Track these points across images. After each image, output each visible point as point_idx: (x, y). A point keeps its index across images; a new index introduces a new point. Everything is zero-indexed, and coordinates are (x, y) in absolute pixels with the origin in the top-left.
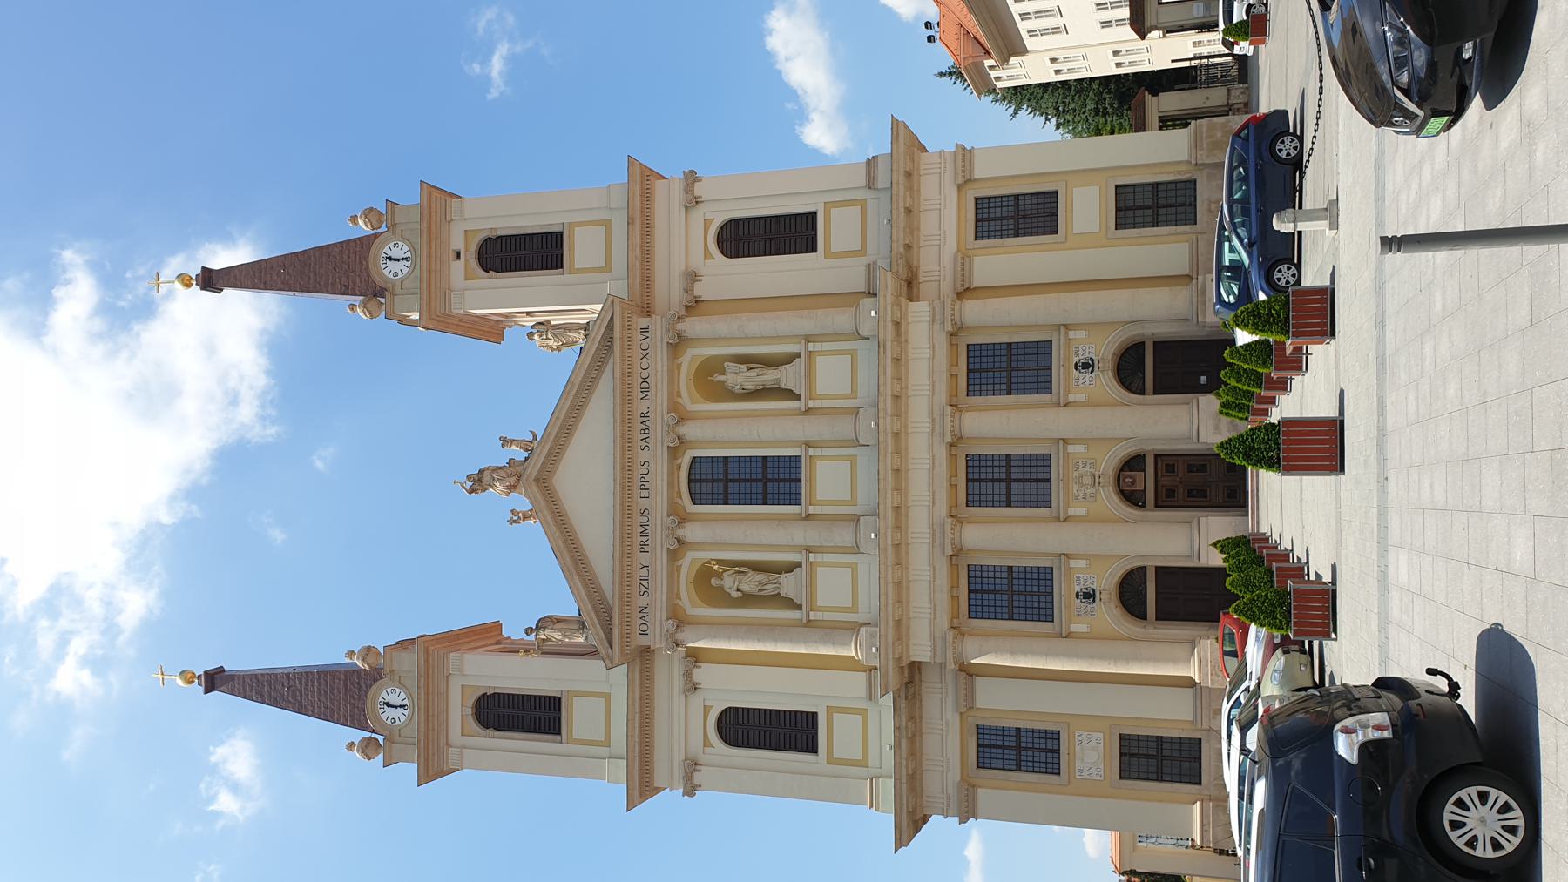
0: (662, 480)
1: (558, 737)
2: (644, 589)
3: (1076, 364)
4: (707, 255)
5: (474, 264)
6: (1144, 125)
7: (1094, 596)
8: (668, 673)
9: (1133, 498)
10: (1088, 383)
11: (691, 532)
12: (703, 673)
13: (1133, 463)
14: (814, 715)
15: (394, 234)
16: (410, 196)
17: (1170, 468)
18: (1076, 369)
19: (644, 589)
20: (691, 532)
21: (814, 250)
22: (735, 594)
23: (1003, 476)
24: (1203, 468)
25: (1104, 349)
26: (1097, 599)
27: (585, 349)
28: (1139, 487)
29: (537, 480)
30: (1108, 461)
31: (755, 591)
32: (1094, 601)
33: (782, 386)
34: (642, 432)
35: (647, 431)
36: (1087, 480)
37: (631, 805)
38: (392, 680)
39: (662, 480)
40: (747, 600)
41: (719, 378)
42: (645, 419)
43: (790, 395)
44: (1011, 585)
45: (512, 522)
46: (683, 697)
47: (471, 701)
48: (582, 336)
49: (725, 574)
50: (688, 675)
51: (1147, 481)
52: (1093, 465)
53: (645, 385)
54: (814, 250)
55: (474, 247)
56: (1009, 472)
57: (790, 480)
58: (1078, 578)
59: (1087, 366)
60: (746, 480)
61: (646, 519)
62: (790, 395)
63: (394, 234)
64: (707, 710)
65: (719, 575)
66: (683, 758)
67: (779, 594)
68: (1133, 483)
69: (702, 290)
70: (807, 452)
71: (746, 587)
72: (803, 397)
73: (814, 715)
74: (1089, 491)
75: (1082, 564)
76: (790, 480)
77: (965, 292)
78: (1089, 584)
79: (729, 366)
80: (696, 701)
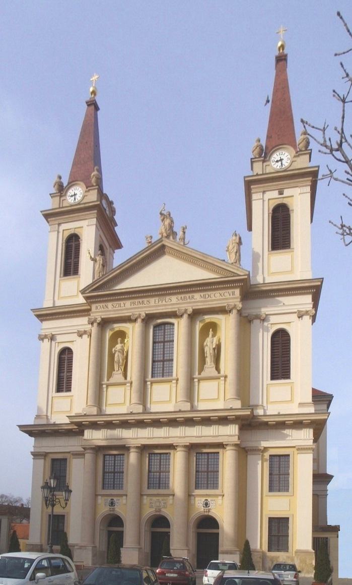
0: (162, 309)
6: (316, 531)
8: (81, 323)
22: (113, 350)
27: (224, 263)
36: (158, 504)
40: (112, 356)
41: (211, 333)
42: (191, 298)
44: (118, 472)
46: (76, 331)
48: (233, 261)
52: (165, 507)
53: (207, 296)
57: (163, 373)
59: (206, 504)
60: (164, 351)
72: (200, 376)
73: (70, 391)
75: (124, 501)
76: (163, 373)
79: (215, 339)
80: (75, 337)
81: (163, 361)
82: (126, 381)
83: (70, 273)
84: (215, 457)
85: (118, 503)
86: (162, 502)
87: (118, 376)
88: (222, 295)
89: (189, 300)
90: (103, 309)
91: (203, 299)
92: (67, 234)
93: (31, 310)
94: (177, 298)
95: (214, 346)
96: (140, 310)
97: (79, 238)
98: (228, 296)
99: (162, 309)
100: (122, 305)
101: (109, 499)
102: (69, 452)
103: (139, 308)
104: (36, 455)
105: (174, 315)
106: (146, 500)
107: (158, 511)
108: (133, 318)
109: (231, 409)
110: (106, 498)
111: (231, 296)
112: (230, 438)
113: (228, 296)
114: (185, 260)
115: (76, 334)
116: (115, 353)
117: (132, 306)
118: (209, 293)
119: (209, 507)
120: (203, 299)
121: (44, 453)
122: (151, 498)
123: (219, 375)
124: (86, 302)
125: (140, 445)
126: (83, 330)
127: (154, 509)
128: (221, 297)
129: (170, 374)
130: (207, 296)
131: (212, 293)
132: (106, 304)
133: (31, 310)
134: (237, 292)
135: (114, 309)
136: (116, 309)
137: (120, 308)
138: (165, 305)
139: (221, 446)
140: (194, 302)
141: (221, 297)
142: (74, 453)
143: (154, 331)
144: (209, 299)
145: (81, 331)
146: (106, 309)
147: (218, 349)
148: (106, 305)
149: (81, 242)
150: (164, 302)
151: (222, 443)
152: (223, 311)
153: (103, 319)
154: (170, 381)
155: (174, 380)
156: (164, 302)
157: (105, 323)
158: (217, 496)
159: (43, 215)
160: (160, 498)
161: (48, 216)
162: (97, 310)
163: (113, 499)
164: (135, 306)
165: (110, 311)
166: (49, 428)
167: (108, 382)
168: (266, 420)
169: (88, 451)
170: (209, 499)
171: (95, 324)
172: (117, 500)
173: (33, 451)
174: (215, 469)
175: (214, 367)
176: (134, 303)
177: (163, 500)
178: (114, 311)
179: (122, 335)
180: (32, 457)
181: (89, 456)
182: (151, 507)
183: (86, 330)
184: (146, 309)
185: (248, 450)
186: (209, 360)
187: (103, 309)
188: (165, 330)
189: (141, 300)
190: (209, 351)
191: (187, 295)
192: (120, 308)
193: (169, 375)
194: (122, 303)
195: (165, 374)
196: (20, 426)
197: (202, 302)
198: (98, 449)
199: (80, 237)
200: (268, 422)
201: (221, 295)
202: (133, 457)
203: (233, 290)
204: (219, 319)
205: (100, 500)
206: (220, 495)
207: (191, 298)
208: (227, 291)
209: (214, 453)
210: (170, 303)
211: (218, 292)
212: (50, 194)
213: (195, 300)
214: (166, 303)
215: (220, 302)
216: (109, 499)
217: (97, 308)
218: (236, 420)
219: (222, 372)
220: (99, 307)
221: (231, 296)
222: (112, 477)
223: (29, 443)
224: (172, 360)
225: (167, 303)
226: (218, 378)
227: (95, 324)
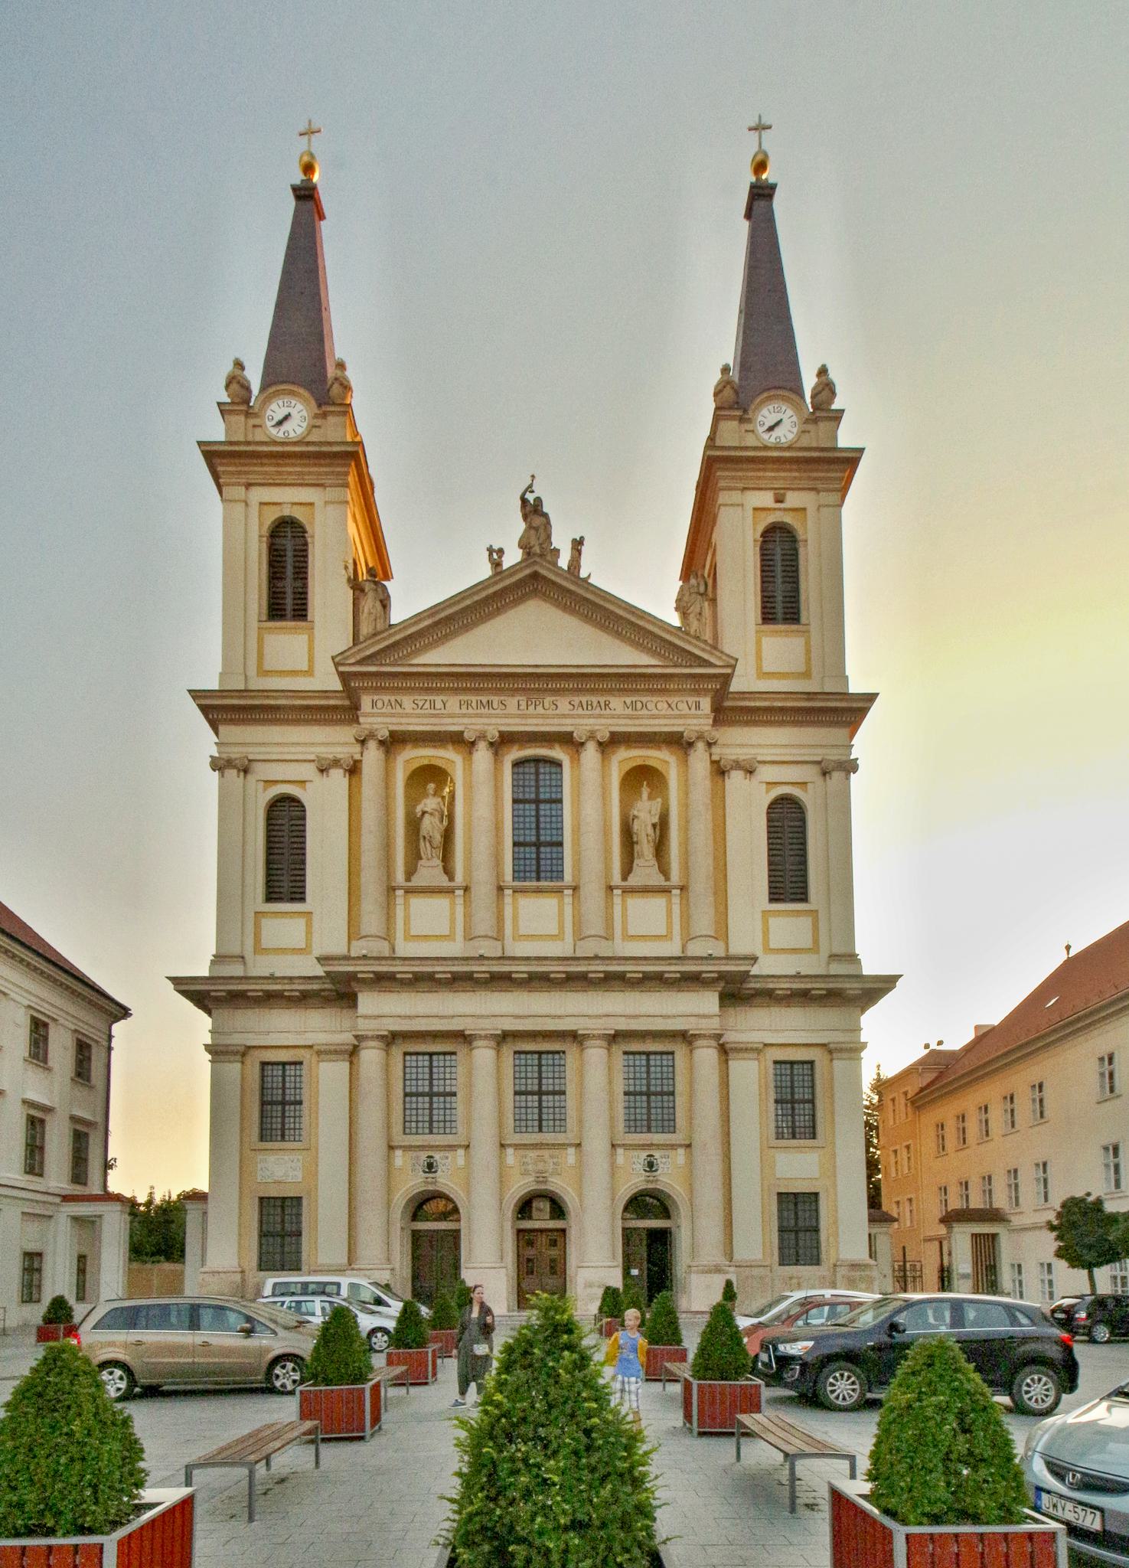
1: (264, 618)
2: (421, 704)
4: (771, 784)
5: (772, 518)
8: (335, 740)
9: (525, 1208)
11: (482, 755)
12: (338, 778)
13: (558, 1209)
14: (303, 900)
15: (807, 421)
16: (846, 438)
17: (553, 1243)
19: (421, 704)
20: (482, 755)
21: (772, 900)
22: (419, 809)
23: (544, 1088)
24: (553, 1271)
25: (670, 1178)
26: (427, 1175)
28: (535, 1214)
29: (535, 576)
30: (559, 1185)
31: (423, 832)
32: (425, 1172)
33: (636, 862)
36: (541, 1166)
37: (195, 694)
38: (316, 416)
40: (414, 825)
42: (603, 705)
43: (627, 871)
44: (439, 1094)
45: (490, 550)
47: (299, 514)
49: (440, 799)
50: (336, 763)
51: (541, 1220)
53: (639, 705)
54: (772, 900)
55: (788, 519)
56: (548, 1093)
57: (538, 872)
58: (447, 1158)
59: (651, 1166)
61: (495, 706)
62: (627, 871)
63: (807, 421)
64: (302, 783)
65: (437, 793)
66: (251, 757)
67: (421, 859)
68: (540, 1210)
69: (736, 778)
70: (568, 888)
71: (427, 819)
73: (303, 900)
74: (530, 1167)
75: (461, 1161)
76: (538, 872)
77: (724, 1051)
80: (308, 771)
82: (667, 883)
83: (285, 615)
87: (430, 872)
88: (674, 706)
89: (598, 711)
91: (629, 711)
92: (272, 515)
96: (486, 721)
97: (305, 532)
98: (686, 711)
99: (626, 725)
100: (439, 705)
101: (423, 1155)
102: (311, 1047)
103: (480, 716)
104: (216, 1052)
108: (469, 736)
109: (710, 957)
112: (704, 1021)
113: (686, 711)
114: (587, 619)
117: (464, 710)
118: (644, 699)
120: (629, 711)
121: (242, 1049)
122: (522, 1152)
123: (667, 883)
125: (499, 1032)
126: (331, 756)
128: (670, 712)
130: (639, 705)
131: (650, 700)
132: (399, 698)
134: (706, 703)
135: (419, 711)
136: (422, 712)
137: (433, 711)
138: (543, 716)
139: (685, 1037)
141: (670, 712)
142: (323, 1048)
144: (644, 712)
145: (326, 759)
146: (399, 710)
147: (662, 826)
149: (309, 540)
150: (540, 710)
151: (576, 1031)
153: (392, 734)
154: (559, 891)
155: (568, 888)
156: (540, 710)
160: (546, 1153)
162: (375, 710)
163: (431, 1157)
164: (470, 711)
165: (407, 716)
166: (258, 987)
167: (409, 884)
172: (441, 1158)
173: (209, 1042)
175: (441, 867)
176: (469, 704)
177: (552, 1157)
178: (418, 716)
180: (209, 1057)
182: (525, 1173)
183: (339, 756)
184: (499, 721)
190: (644, 830)
191: (594, 699)
192: (433, 711)
194: (438, 699)
195: (542, 875)
196: (178, 982)
199: (308, 528)
201: (670, 706)
207: (603, 705)
208: (684, 699)
210: (554, 712)
211: (664, 699)
213: (613, 712)
215: (672, 721)
216: (423, 1156)
217: (374, 704)
219: (459, 878)
220: (380, 704)
221: (693, 711)
222: (427, 1106)
223: (201, 1024)
225: (548, 712)
227: (372, 745)
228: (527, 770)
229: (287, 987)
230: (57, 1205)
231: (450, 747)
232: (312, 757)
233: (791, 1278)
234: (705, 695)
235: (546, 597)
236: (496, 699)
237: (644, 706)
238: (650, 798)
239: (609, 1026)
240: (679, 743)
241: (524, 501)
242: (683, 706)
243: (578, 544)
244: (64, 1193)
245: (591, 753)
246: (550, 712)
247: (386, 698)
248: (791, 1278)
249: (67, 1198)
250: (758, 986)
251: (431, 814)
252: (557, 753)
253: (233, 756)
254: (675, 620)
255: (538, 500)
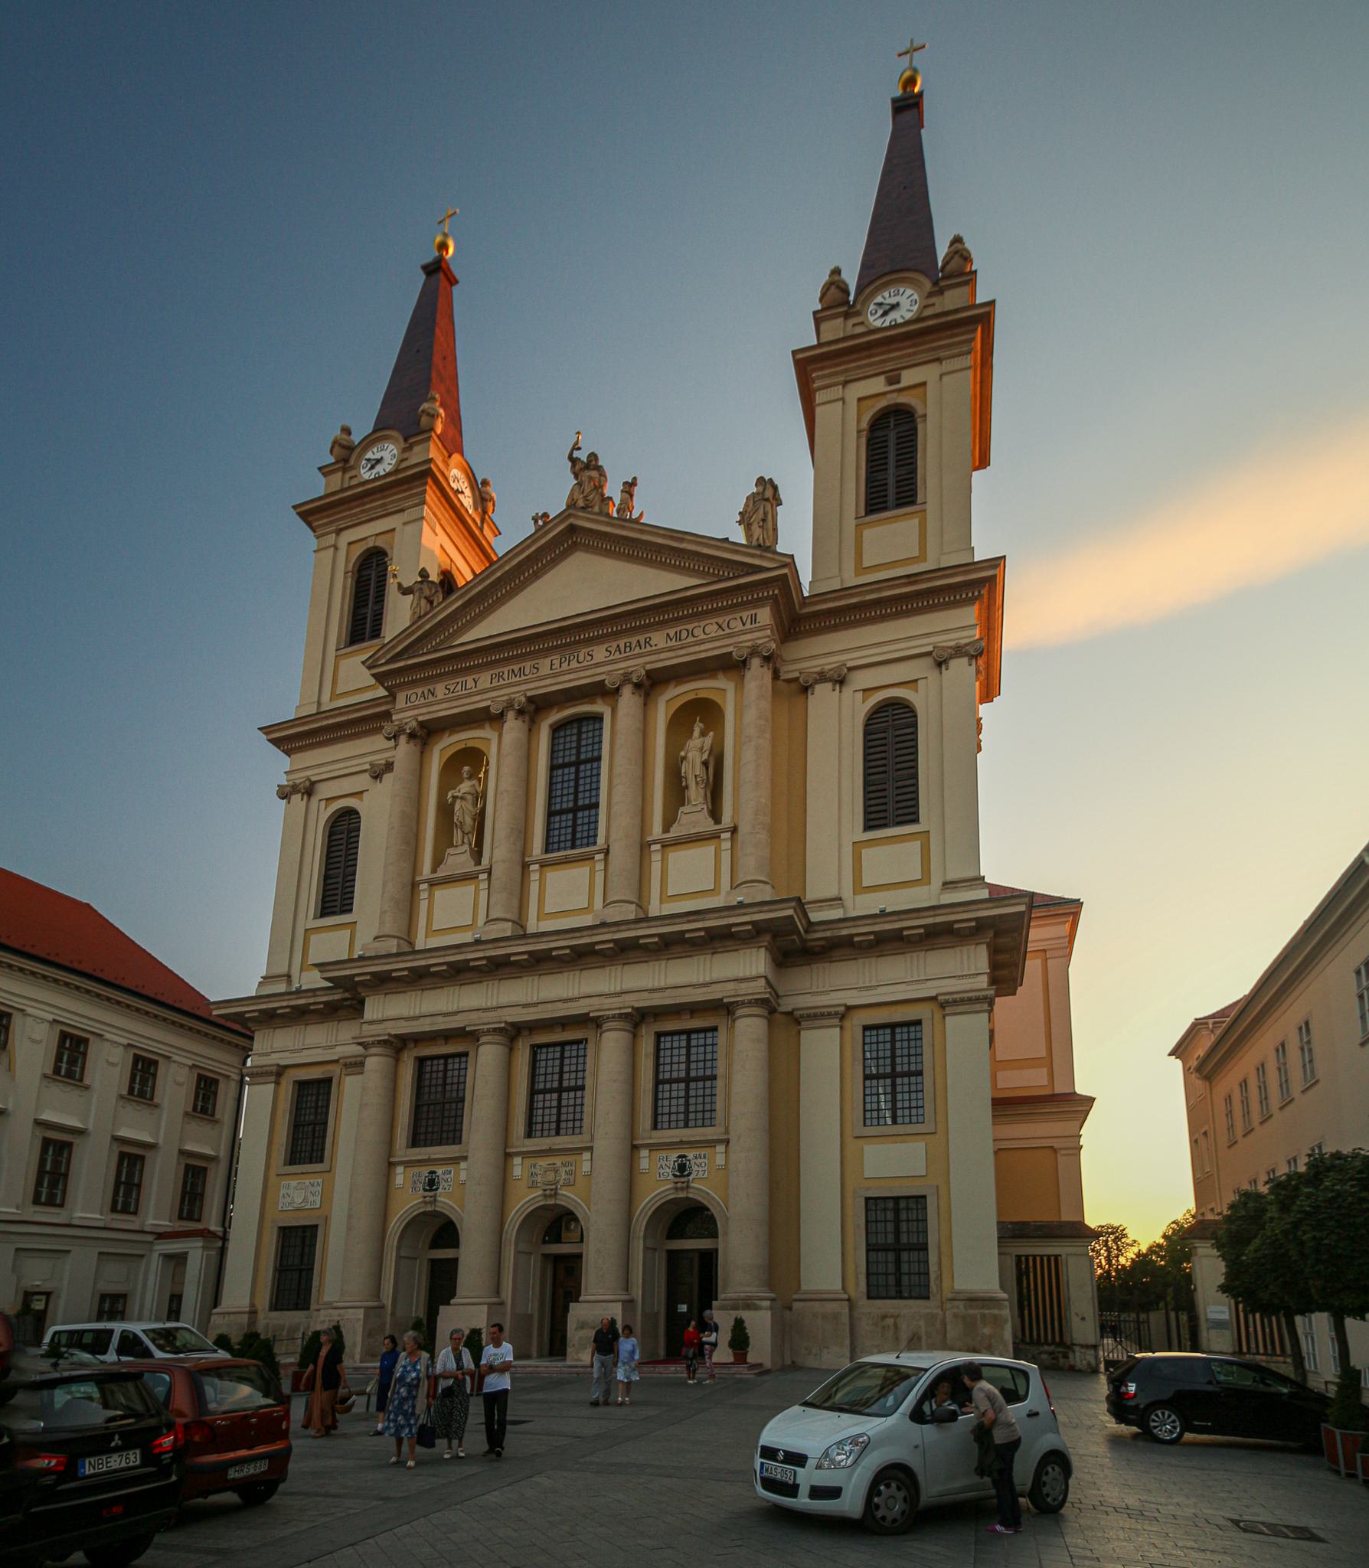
0: (570, 681)
3: (684, 1156)
7: (431, 1190)
10: (662, 1171)
18: (679, 1157)
22: (450, 794)
32: (425, 1190)
34: (628, 645)
35: (628, 649)
36: (551, 1176)
38: (404, 450)
39: (570, 681)
40: (445, 811)
52: (568, 1184)
57: (574, 840)
58: (450, 1173)
59: (682, 1168)
66: (313, 779)
76: (574, 840)
78: (443, 1184)
81: (575, 810)
84: (709, 1041)
85: (446, 1181)
86: (563, 1171)
88: (725, 626)
90: (422, 701)
91: (673, 643)
92: (358, 551)
93: (259, 729)
94: (607, 650)
95: (705, 756)
98: (740, 627)
101: (425, 1171)
102: (336, 1061)
105: (600, 691)
106: (518, 1167)
107: (550, 1196)
108: (495, 709)
110: (416, 1170)
111: (748, 626)
112: (743, 985)
113: (740, 627)
115: (367, 775)
116: (453, 804)
118: (690, 627)
119: (689, 1175)
121: (274, 1069)
122: (532, 1161)
124: (387, 694)
127: (540, 1192)
129: (591, 840)
130: (684, 634)
133: (259, 729)
134: (765, 615)
135: (451, 695)
137: (464, 692)
138: (576, 670)
139: (725, 1009)
140: (650, 653)
143: (553, 739)
144: (691, 639)
146: (431, 699)
147: (715, 766)
148: (429, 690)
150: (574, 664)
152: (731, 665)
154: (590, 858)
156: (574, 664)
157: (426, 733)
158: (711, 1143)
159: (300, 514)
160: (558, 1161)
161: (311, 514)
162: (409, 704)
163: (434, 1172)
164: (502, 682)
167: (435, 875)
168: (845, 932)
169: (373, 1050)
170: (690, 1155)
171: (403, 739)
172: (444, 1174)
174: (708, 1072)
176: (500, 676)
179: (471, 759)
181: (375, 1063)
182: (533, 1186)
185: (802, 1016)
186: (696, 794)
187: (422, 701)
188: (580, 733)
189: (516, 668)
191: (634, 640)
193: (588, 845)
194: (470, 680)
197: (670, 649)
198: (398, 1045)
200: (852, 936)
202: (487, 1057)
203: (753, 612)
204: (719, 688)
205: (400, 1176)
206: (720, 1141)
208: (738, 616)
209: (705, 1030)
212: (320, 469)
213: (654, 648)
214: (579, 665)
216: (425, 1171)
218: (757, 932)
224: (596, 806)
225: (582, 665)
226: (715, 837)
227: (403, 739)
228: (568, 732)
229: (312, 1000)
230: (151, 1243)
231: (487, 726)
232: (367, 767)
233: (884, 1317)
234: (763, 606)
235: (588, 549)
236: (528, 665)
237: (689, 633)
238: (703, 734)
239: (626, 1005)
240: (731, 665)
241: (573, 460)
242: (737, 626)
243: (629, 487)
244: (161, 1230)
245: (628, 700)
246: (585, 664)
247: (419, 691)
248: (884, 1317)
249: (161, 1236)
250: (828, 934)
251: (462, 798)
252: (599, 707)
253: (298, 782)
254: (739, 536)
255: (593, 456)
